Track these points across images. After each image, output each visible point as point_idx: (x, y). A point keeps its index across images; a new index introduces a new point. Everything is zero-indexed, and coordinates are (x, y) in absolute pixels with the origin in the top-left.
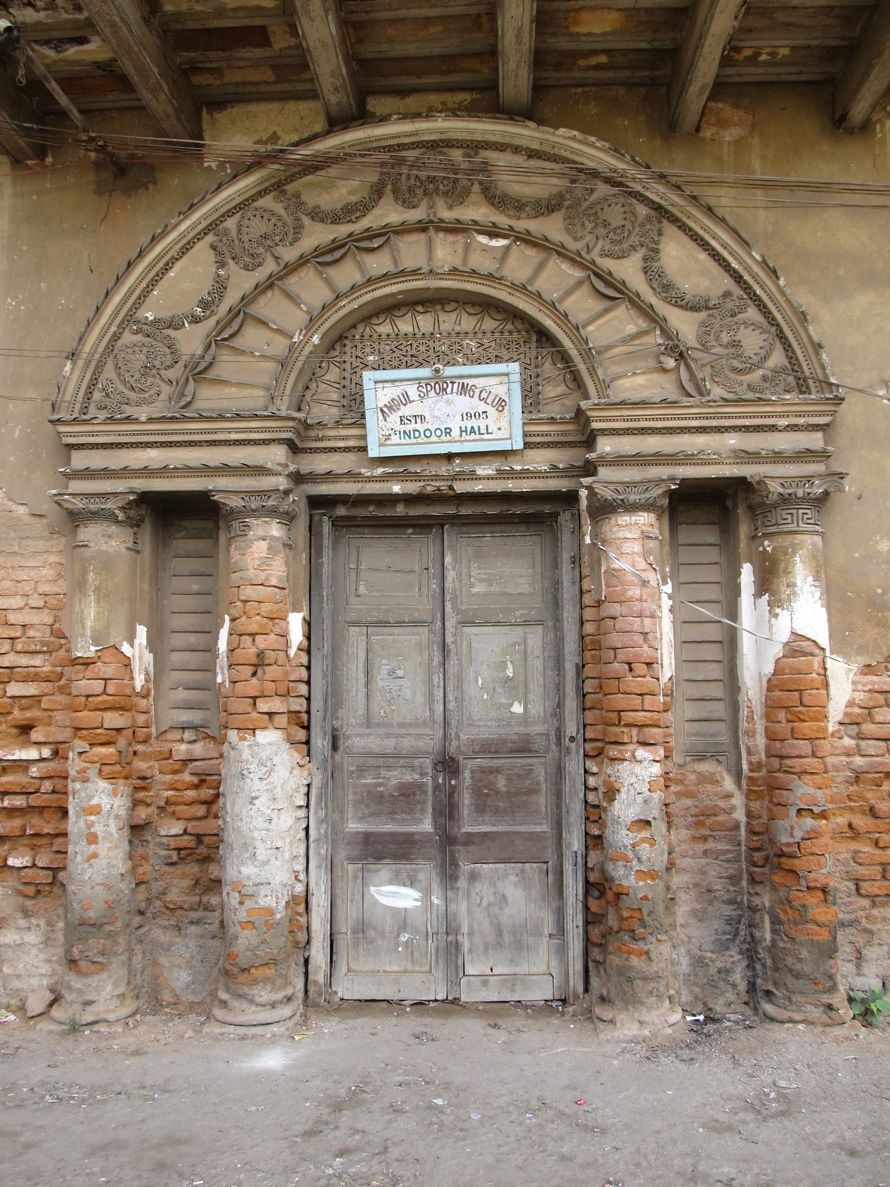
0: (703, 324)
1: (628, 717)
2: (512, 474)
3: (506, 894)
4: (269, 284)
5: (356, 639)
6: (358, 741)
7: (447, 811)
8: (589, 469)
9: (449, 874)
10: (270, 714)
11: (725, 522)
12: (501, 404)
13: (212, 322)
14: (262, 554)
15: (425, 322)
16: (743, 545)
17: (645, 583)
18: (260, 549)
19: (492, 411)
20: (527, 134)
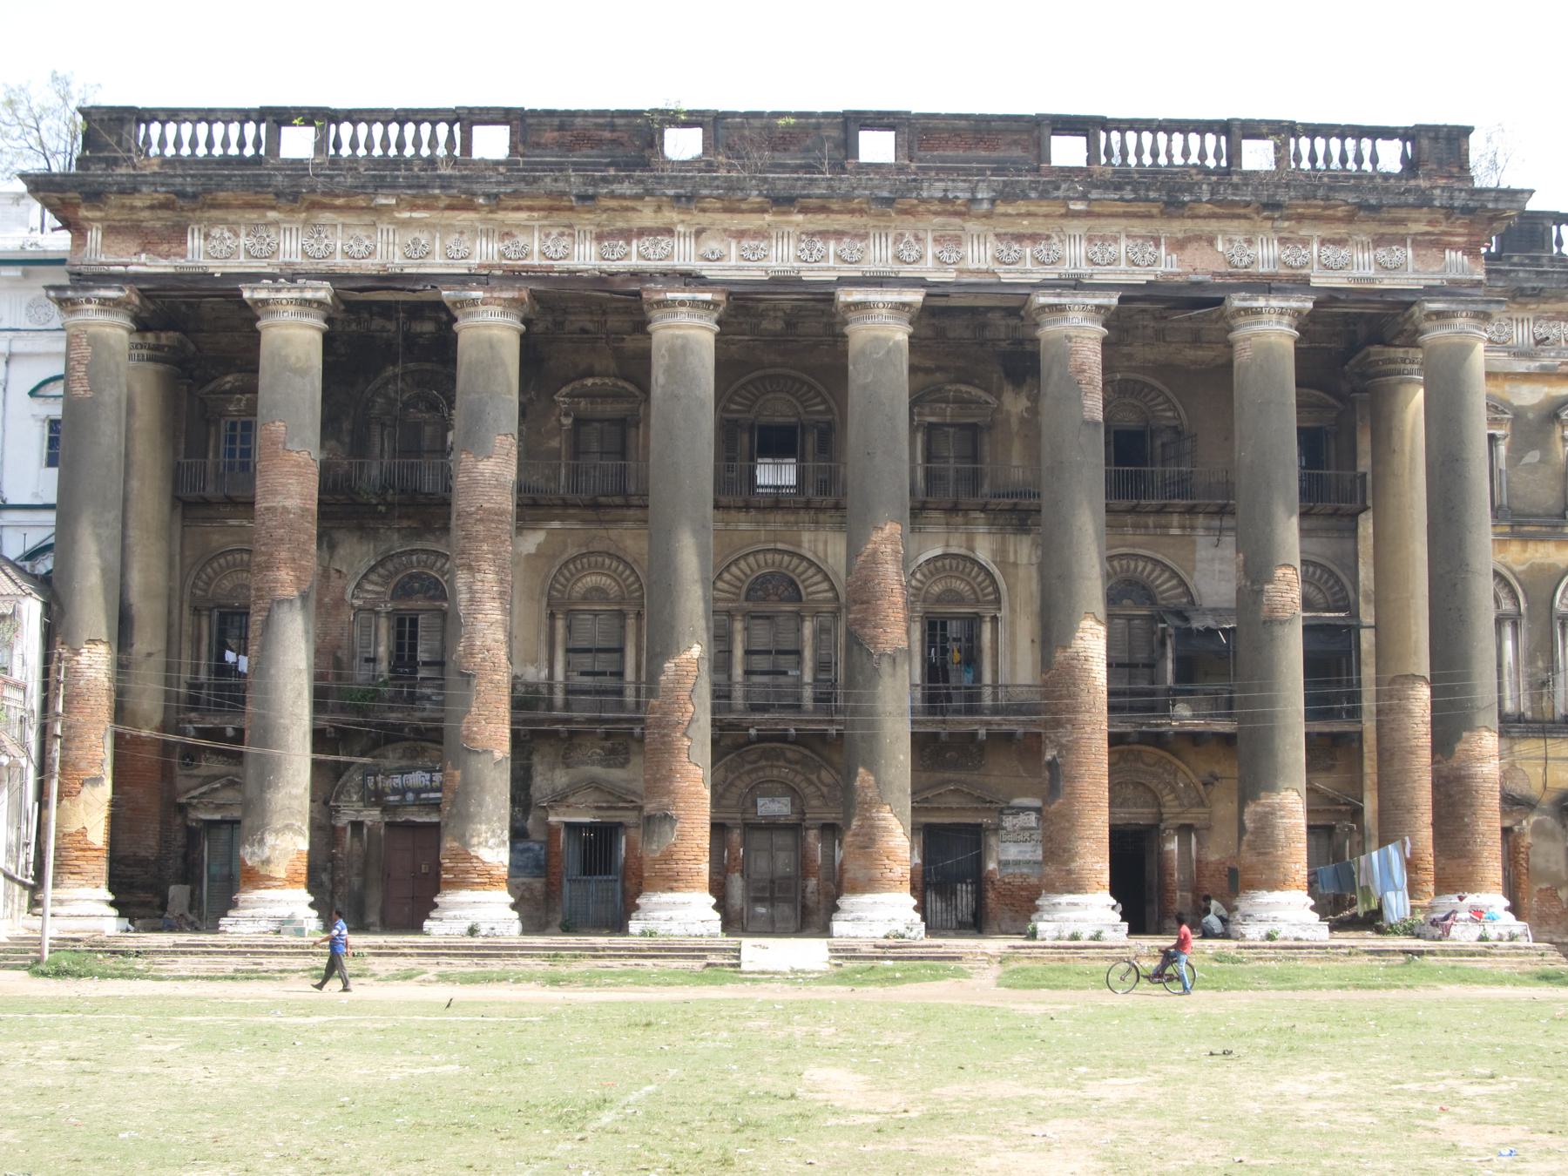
3: (785, 910)
7: (772, 892)
9: (772, 905)
14: (736, 836)
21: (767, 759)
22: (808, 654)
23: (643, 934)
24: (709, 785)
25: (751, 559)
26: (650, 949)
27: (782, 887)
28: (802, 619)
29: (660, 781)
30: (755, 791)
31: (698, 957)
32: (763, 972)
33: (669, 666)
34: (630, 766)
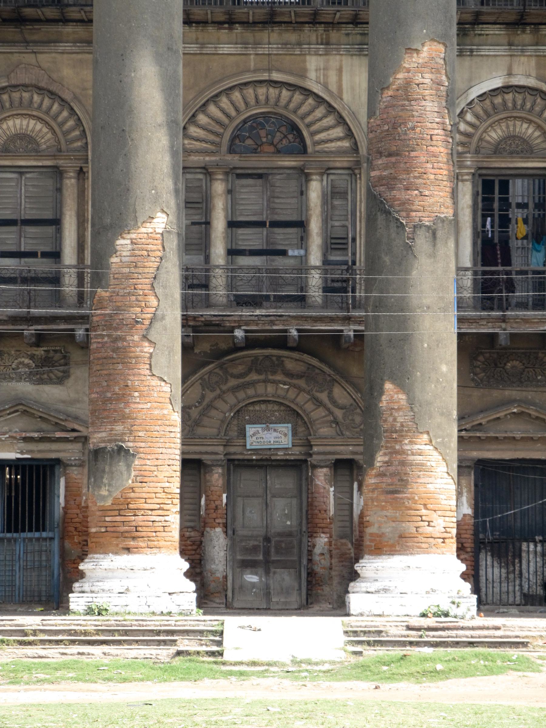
0: (344, 414)
1: (319, 525)
2: (288, 454)
3: (284, 578)
4: (219, 396)
5: (240, 501)
6: (241, 532)
7: (267, 553)
8: (311, 455)
9: (267, 572)
10: (219, 523)
11: (351, 470)
12: (285, 435)
13: (201, 408)
14: (216, 477)
15: (263, 407)
16: (355, 477)
17: (325, 488)
18: (216, 476)
19: (283, 436)
20: (295, 355)
21: (259, 372)
22: (315, 226)
23: (90, 611)
24: (178, 407)
25: (236, 95)
26: (98, 632)
27: (282, 545)
28: (307, 178)
29: (112, 401)
30: (242, 415)
31: (165, 642)
32: (254, 664)
33: (123, 243)
34: (70, 382)
